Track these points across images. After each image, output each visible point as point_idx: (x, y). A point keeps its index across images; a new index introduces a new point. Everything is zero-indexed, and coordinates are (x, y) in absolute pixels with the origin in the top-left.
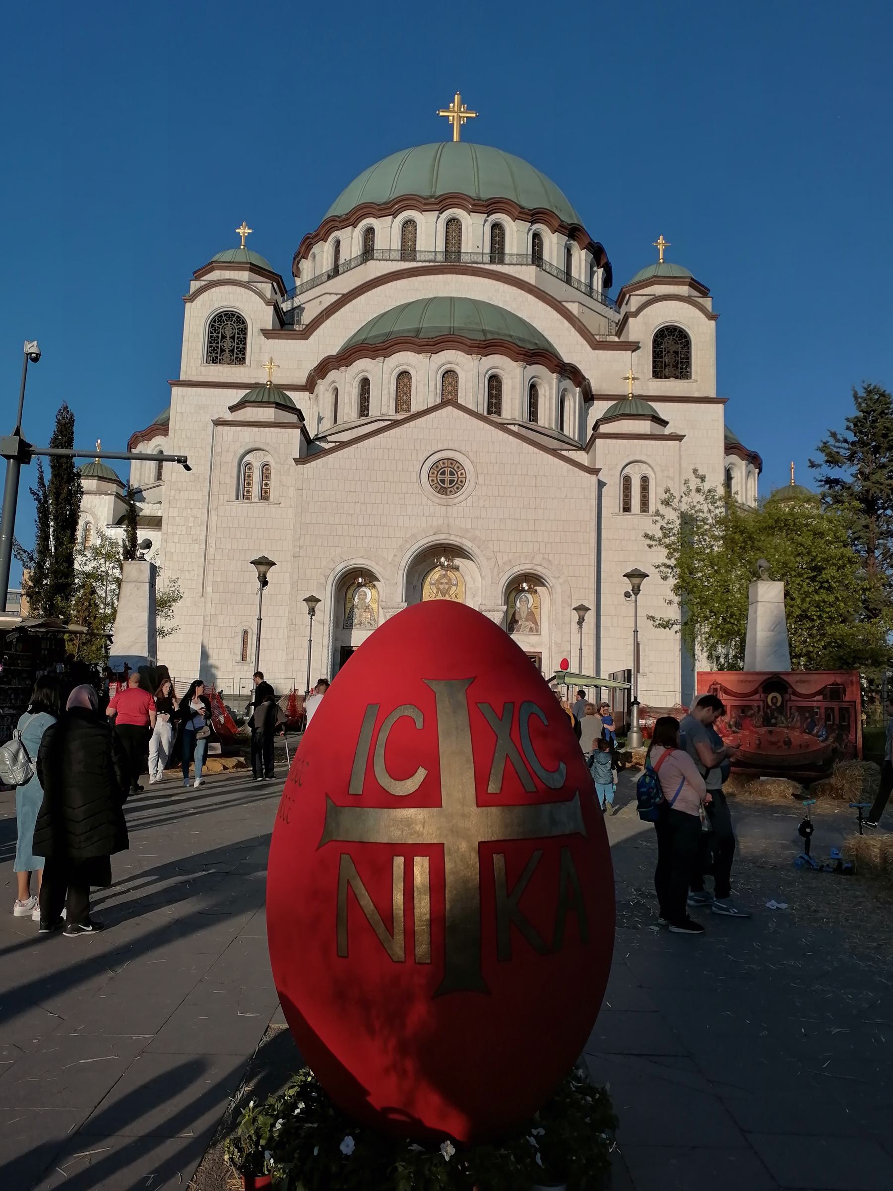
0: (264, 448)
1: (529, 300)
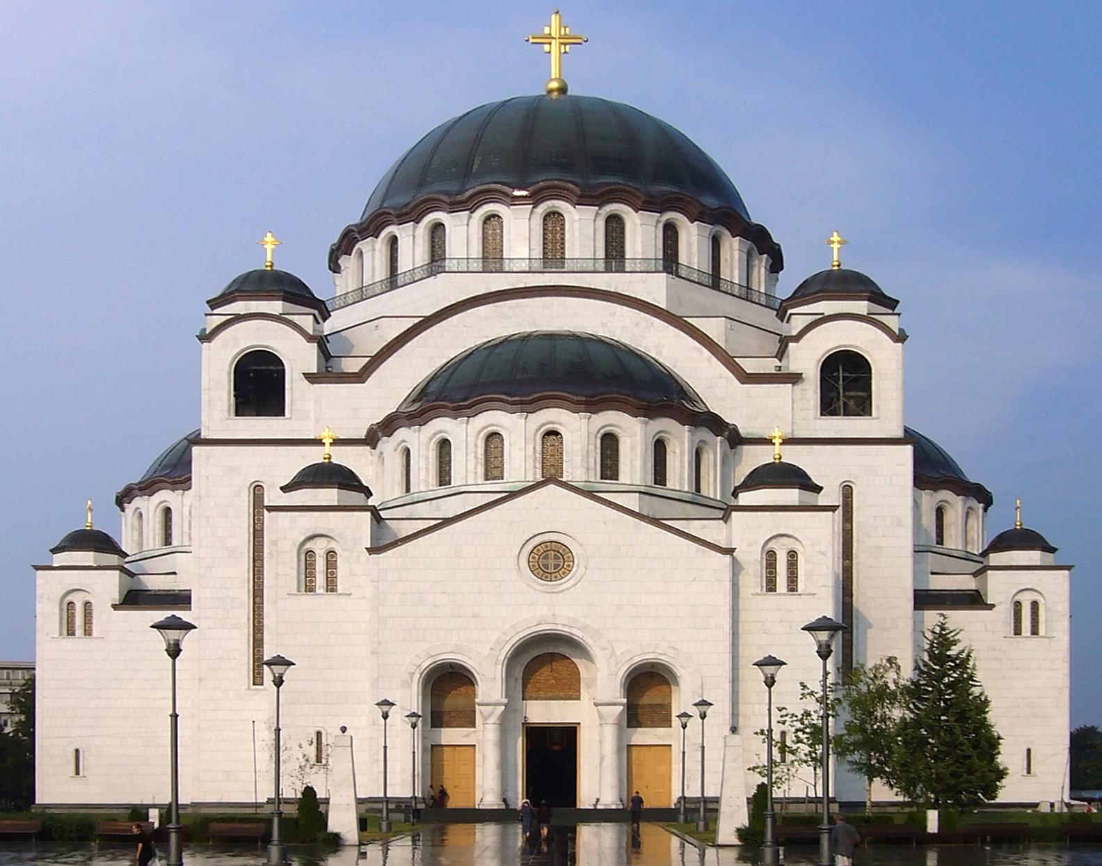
0: (328, 534)
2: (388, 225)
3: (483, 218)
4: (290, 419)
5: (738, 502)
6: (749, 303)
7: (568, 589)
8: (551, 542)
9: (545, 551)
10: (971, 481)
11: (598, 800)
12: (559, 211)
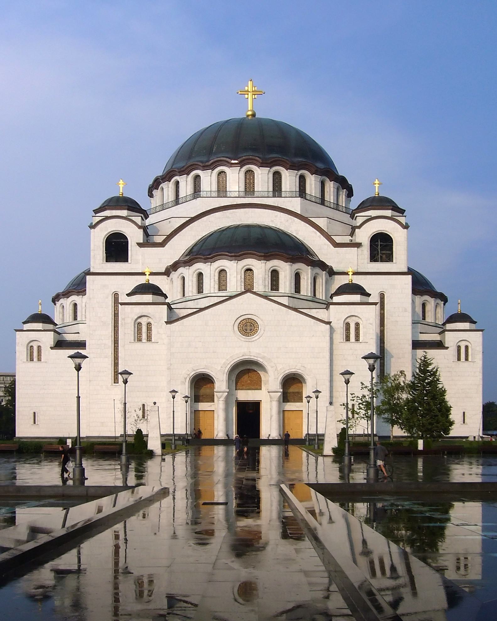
0: (148, 315)
1: (295, 220)
2: (175, 176)
3: (218, 173)
4: (131, 263)
5: (333, 301)
6: (338, 211)
7: (256, 340)
8: (248, 319)
9: (246, 323)
10: (438, 291)
11: (269, 435)
12: (252, 170)
